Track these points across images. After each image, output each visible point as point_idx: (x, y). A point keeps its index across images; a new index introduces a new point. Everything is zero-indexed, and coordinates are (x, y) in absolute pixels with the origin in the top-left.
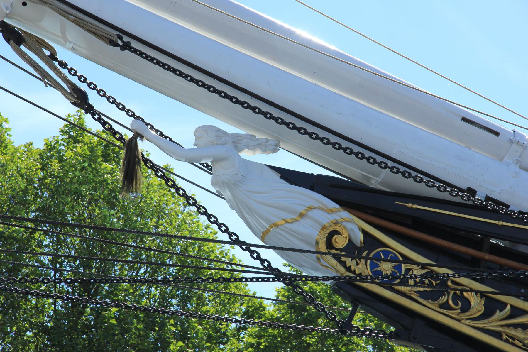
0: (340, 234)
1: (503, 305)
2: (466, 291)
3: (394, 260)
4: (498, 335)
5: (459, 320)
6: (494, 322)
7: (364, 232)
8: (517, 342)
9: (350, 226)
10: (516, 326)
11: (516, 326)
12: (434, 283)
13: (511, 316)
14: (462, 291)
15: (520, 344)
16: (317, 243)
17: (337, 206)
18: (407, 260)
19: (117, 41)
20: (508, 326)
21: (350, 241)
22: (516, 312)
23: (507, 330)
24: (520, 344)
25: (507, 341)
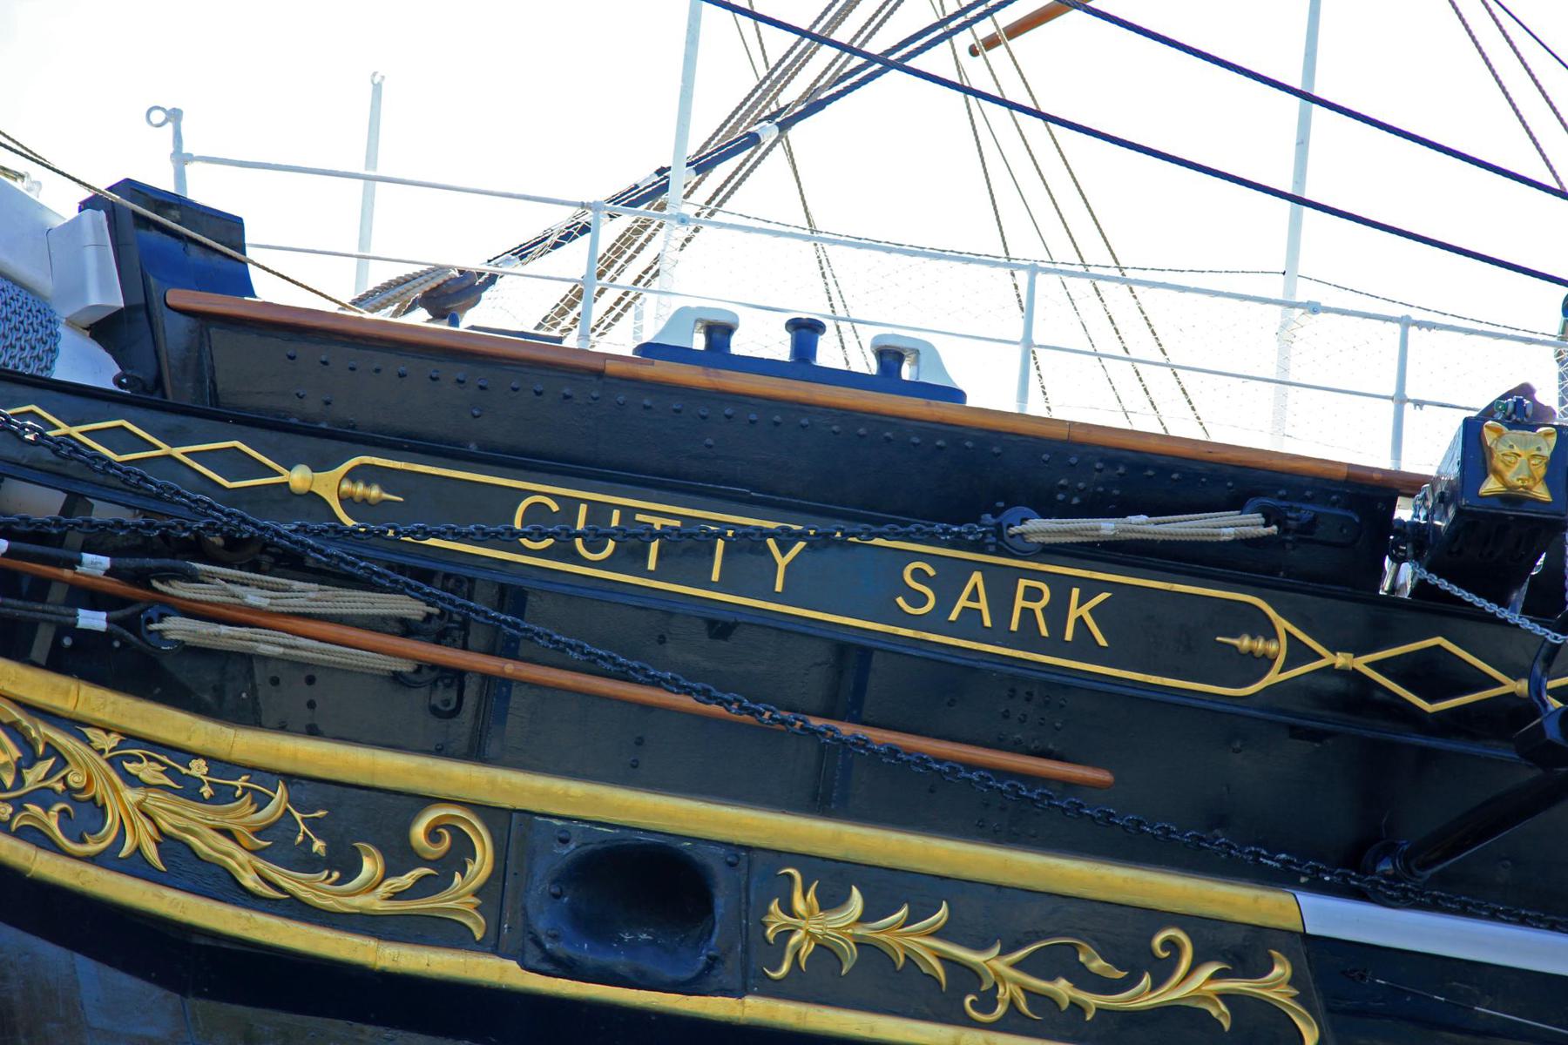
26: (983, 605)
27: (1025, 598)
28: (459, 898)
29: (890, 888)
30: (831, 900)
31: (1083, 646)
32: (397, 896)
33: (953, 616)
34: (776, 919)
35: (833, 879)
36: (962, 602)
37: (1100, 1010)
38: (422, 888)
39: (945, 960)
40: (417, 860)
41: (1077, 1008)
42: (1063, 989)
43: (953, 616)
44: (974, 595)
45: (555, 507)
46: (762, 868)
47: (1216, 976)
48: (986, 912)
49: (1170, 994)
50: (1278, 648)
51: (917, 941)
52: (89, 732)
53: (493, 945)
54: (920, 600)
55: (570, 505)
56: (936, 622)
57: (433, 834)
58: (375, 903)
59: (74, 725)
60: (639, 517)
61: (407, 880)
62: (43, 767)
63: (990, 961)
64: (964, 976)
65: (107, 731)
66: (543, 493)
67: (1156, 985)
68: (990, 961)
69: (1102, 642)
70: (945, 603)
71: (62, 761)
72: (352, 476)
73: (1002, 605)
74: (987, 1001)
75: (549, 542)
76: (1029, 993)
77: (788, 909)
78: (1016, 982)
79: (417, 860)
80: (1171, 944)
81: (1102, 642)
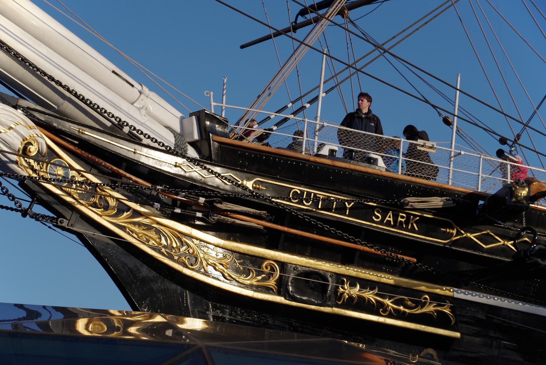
0: (32, 145)
1: (129, 208)
2: (108, 196)
3: (64, 167)
4: (122, 228)
5: (101, 216)
6: (122, 220)
7: (49, 147)
8: (134, 235)
9: (40, 140)
10: (134, 224)
11: (134, 224)
12: (88, 188)
13: (132, 217)
14: (105, 196)
15: (136, 236)
16: (19, 151)
17: (34, 125)
18: (71, 168)
19: (215, 127)
20: (131, 223)
21: (39, 151)
22: (137, 214)
23: (130, 226)
24: (136, 236)
25: (129, 234)
26: (391, 219)
27: (401, 218)
28: (272, 283)
29: (366, 284)
30: (353, 285)
31: (413, 230)
32: (258, 281)
33: (385, 222)
34: (341, 290)
35: (353, 281)
36: (387, 218)
37: (409, 313)
38: (264, 279)
39: (376, 300)
40: (263, 273)
41: (404, 312)
42: (402, 308)
43: (385, 222)
44: (389, 218)
45: (299, 192)
46: (339, 278)
47: (434, 306)
48: (384, 289)
49: (425, 310)
50: (455, 232)
51: (370, 295)
52: (193, 240)
53: (279, 294)
54: (378, 217)
55: (303, 192)
56: (381, 223)
57: (267, 268)
58: (254, 282)
59: (191, 237)
60: (318, 195)
61: (259, 278)
62: (184, 248)
63: (387, 302)
64: (381, 305)
65: (197, 240)
66: (297, 189)
67: (422, 308)
68: (387, 302)
69: (417, 229)
70: (384, 218)
71: (189, 246)
72: (255, 183)
73: (395, 221)
74: (385, 311)
75: (297, 201)
76: (394, 309)
77: (343, 288)
78: (391, 306)
79: (263, 273)
80: (426, 299)
81: (417, 229)
